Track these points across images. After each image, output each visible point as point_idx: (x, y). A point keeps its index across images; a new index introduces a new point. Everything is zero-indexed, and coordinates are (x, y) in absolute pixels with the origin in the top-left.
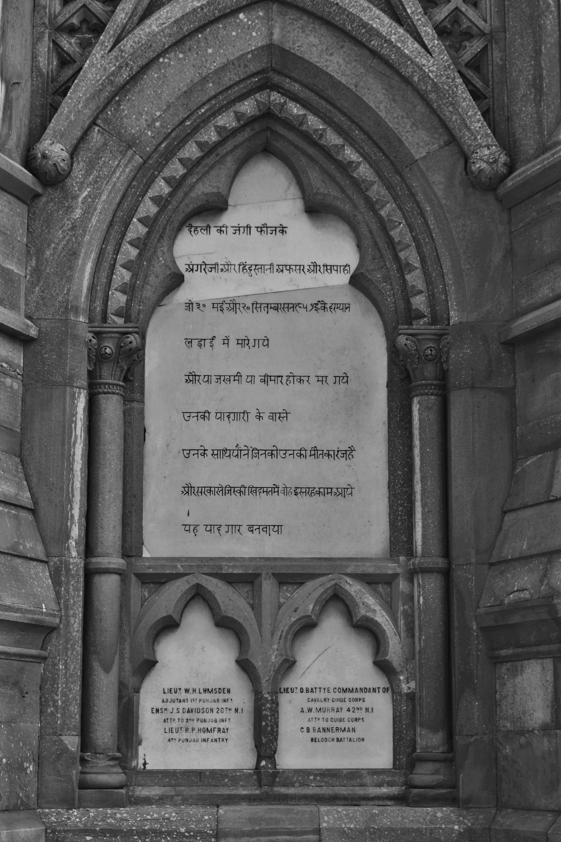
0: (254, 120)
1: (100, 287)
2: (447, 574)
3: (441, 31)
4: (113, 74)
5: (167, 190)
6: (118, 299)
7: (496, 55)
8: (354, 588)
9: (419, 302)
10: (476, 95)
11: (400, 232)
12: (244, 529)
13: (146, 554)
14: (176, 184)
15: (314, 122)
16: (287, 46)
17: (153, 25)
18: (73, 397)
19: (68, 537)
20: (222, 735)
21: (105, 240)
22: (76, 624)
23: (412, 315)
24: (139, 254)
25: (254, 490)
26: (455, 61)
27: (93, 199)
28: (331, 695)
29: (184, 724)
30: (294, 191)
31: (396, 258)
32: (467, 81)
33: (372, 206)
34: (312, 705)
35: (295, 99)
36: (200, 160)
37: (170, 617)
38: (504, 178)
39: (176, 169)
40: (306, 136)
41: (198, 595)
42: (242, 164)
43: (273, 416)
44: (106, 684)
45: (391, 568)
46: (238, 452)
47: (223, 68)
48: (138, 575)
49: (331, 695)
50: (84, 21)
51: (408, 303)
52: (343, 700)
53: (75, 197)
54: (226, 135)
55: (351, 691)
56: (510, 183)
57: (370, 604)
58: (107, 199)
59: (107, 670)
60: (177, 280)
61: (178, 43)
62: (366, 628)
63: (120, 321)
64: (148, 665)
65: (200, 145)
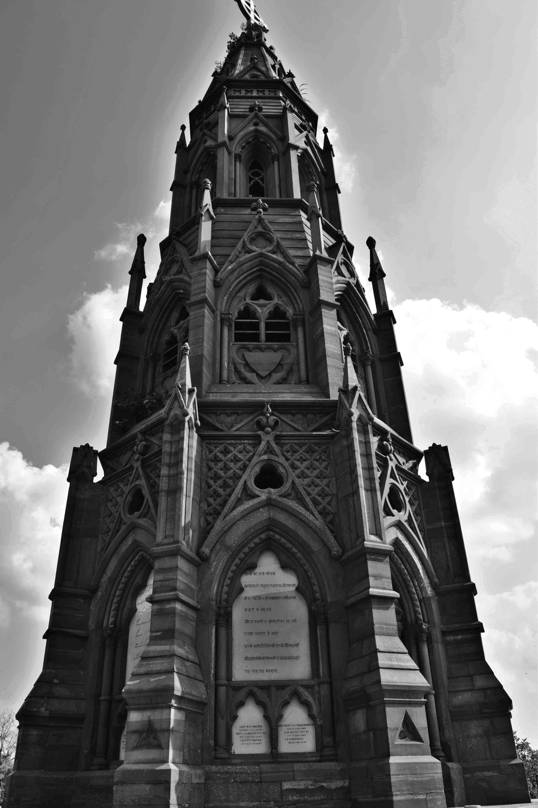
0: (265, 540)
1: (219, 593)
2: (331, 684)
3: (320, 513)
4: (223, 527)
5: (239, 562)
6: (224, 596)
7: (337, 519)
8: (301, 690)
9: (318, 595)
10: (332, 531)
11: (311, 573)
12: (265, 671)
13: (233, 680)
14: (241, 560)
15: (283, 540)
16: (275, 518)
17: (235, 513)
18: (212, 628)
19: (210, 673)
20: (259, 742)
21: (221, 578)
22: (213, 702)
23: (315, 600)
24: (231, 582)
25: (267, 658)
26: (325, 521)
27: (217, 565)
28: (295, 727)
29: (247, 738)
30: (277, 561)
31: (310, 581)
32: (329, 527)
33: (302, 566)
34: (288, 730)
35: (277, 533)
36: (249, 552)
37: (242, 701)
38: (341, 556)
39: (242, 555)
40: (281, 545)
41: (251, 694)
42: (261, 553)
43: (273, 633)
44: (222, 723)
45: (312, 682)
46: (262, 645)
47: (256, 525)
48: (231, 687)
49: (295, 727)
50: (214, 512)
51: (314, 596)
52: (299, 729)
53: (212, 565)
54: (257, 545)
55: (301, 725)
56: (343, 558)
57: (306, 695)
58: (221, 565)
59: (223, 719)
60: (242, 590)
61: (242, 518)
62: (305, 704)
63: (225, 603)
64: (235, 717)
65: (249, 548)
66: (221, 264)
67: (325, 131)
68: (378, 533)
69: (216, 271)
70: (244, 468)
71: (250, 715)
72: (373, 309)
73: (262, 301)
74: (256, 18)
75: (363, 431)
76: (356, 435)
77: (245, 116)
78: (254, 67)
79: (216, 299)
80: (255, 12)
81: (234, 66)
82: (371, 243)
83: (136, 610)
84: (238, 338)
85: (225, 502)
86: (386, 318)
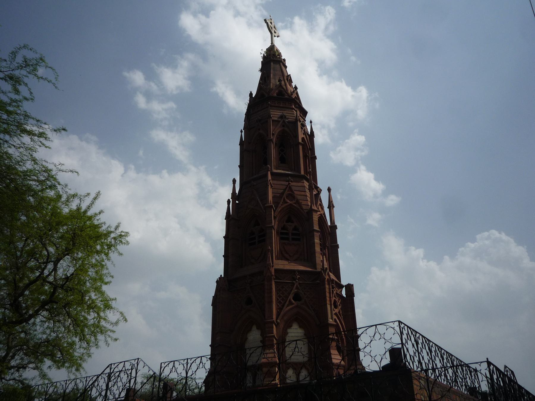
62: (307, 369)
66: (276, 207)
67: (311, 122)
68: (332, 319)
69: (274, 211)
70: (289, 294)
71: (290, 372)
72: (329, 224)
73: (290, 224)
74: (275, 32)
75: (329, 284)
76: (327, 286)
77: (279, 121)
78: (280, 85)
79: (275, 224)
80: (274, 27)
81: (269, 76)
82: (329, 190)
83: (247, 339)
84: (281, 239)
85: (283, 306)
86: (334, 227)
